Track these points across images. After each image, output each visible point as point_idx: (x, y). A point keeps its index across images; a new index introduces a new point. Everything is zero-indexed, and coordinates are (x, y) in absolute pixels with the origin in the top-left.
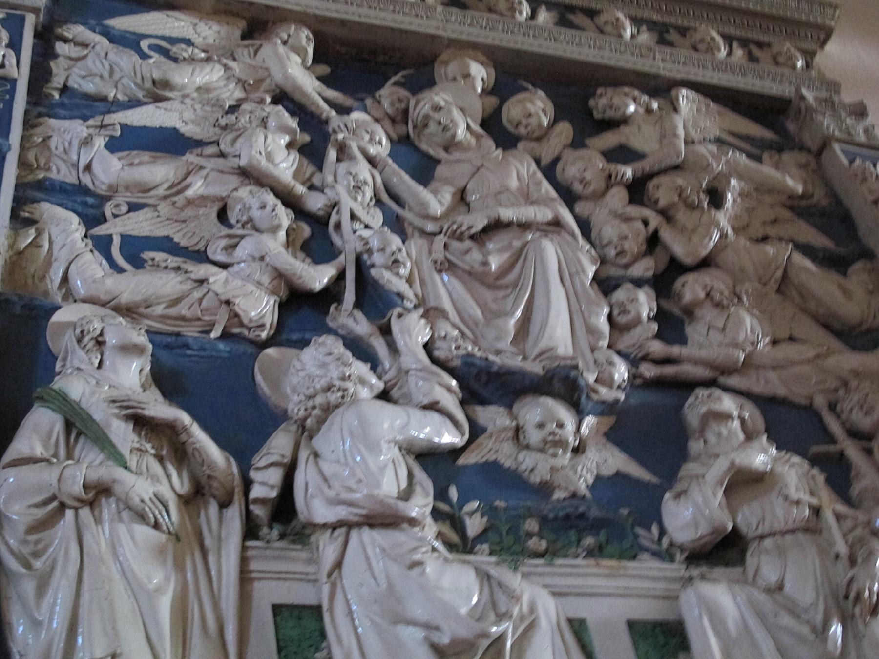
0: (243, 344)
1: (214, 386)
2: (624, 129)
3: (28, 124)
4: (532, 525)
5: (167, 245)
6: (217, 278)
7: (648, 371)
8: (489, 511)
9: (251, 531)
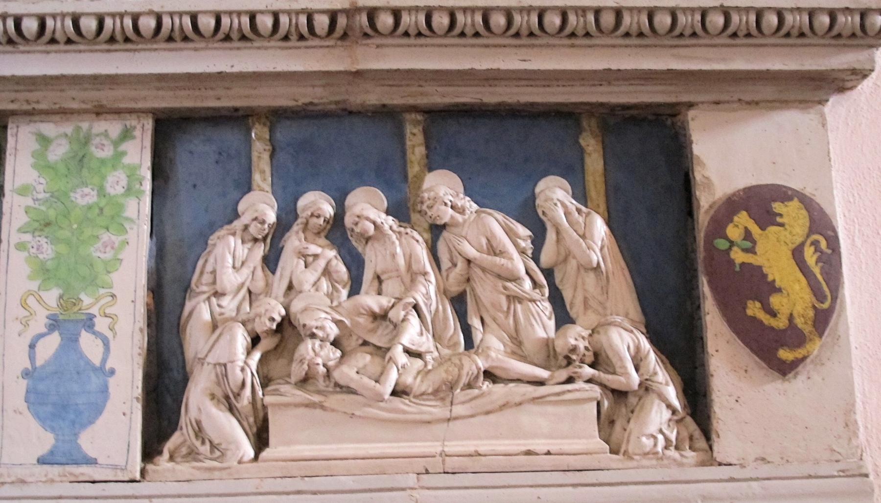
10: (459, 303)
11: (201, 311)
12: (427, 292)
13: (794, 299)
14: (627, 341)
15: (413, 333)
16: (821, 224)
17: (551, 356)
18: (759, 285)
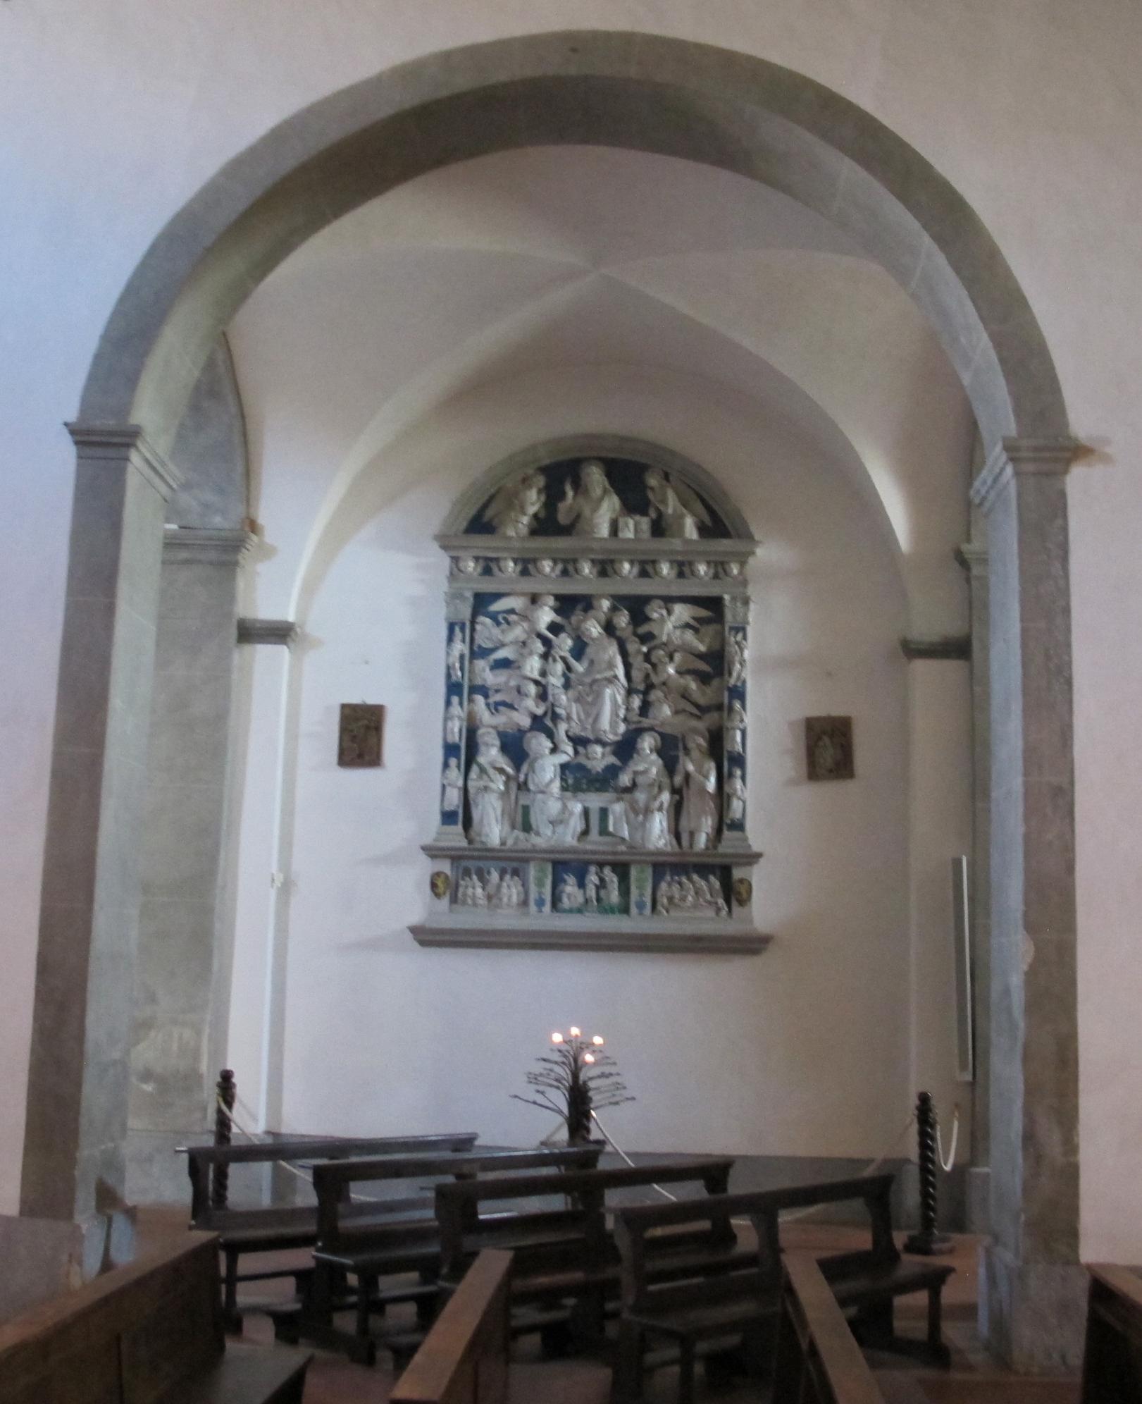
0: (521, 732)
1: (514, 748)
2: (652, 624)
3: (471, 662)
4: (584, 781)
5: (504, 704)
6: (515, 715)
7: (634, 726)
8: (575, 778)
9: (519, 788)
10: (696, 893)
11: (659, 894)
12: (692, 892)
13: (745, 895)
14: (721, 901)
15: (690, 898)
16: (750, 885)
17: (710, 903)
18: (739, 893)
